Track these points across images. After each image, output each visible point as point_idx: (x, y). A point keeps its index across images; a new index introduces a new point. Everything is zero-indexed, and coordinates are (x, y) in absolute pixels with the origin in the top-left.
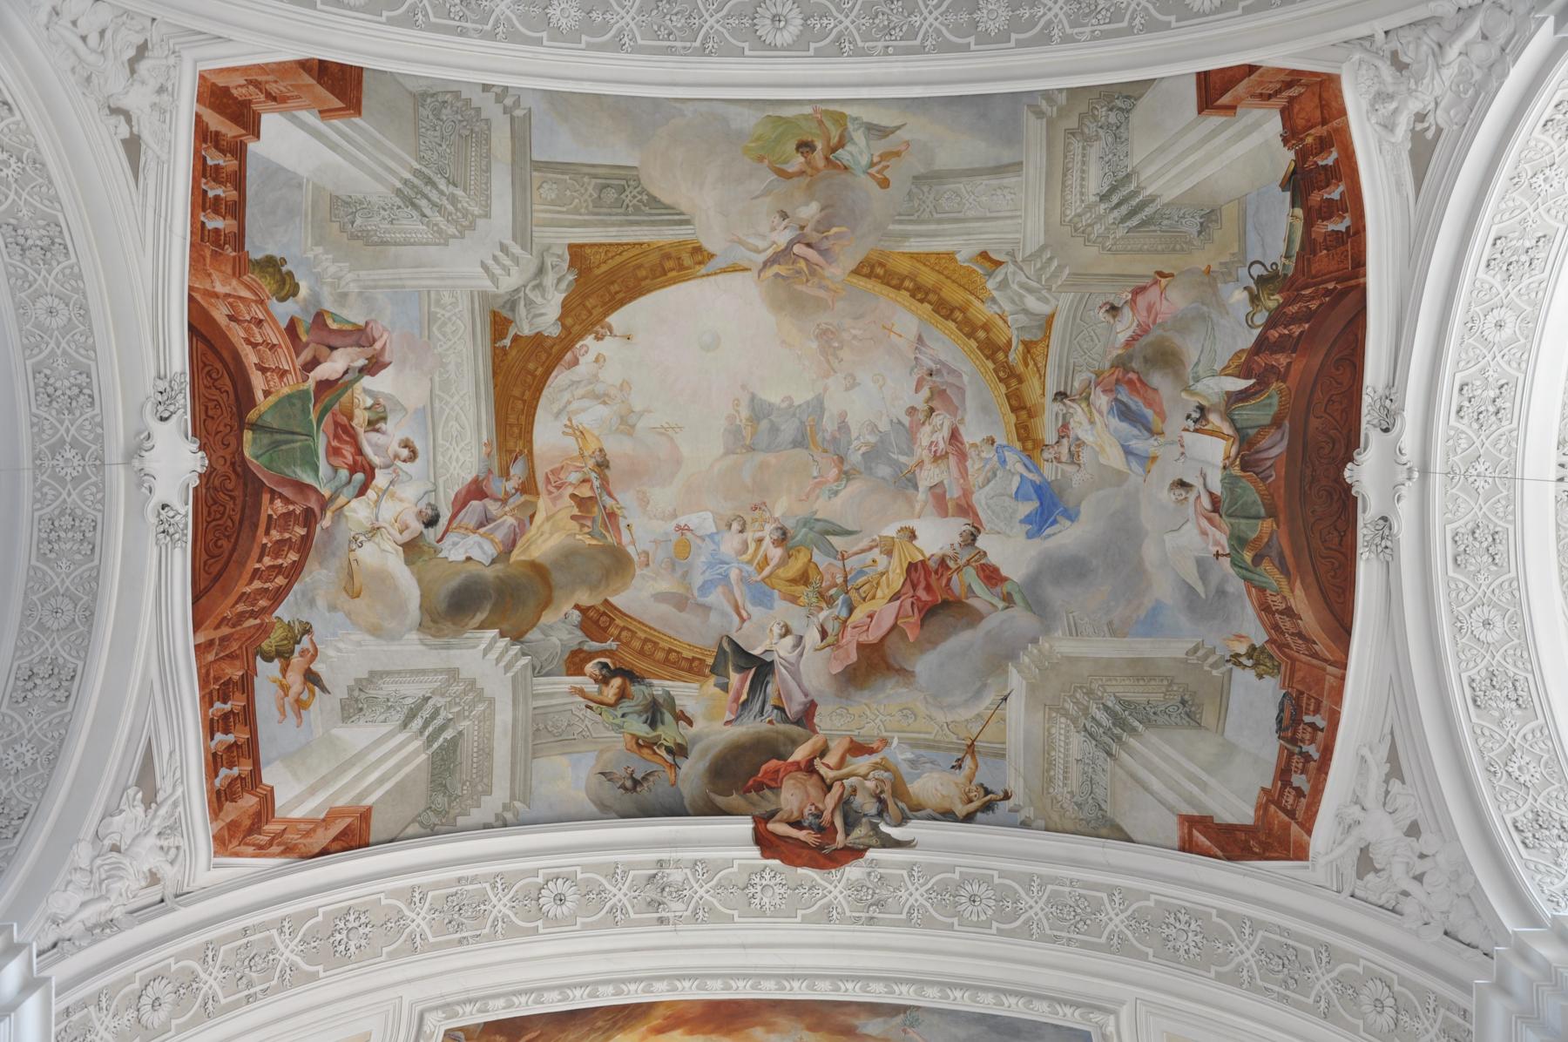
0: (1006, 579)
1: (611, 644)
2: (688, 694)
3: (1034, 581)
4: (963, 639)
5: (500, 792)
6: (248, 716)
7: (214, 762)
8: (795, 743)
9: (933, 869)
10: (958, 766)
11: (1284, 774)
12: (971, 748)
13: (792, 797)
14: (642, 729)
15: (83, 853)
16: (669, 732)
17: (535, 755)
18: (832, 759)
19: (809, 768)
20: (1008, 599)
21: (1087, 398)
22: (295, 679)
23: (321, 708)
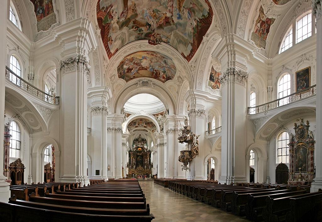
0: (174, 22)
1: (136, 24)
2: (143, 28)
3: (177, 24)
4: (170, 26)
8: (153, 33)
9: (162, 47)
10: (166, 38)
12: (168, 37)
13: (152, 38)
14: (139, 32)
16: (141, 32)
18: (156, 35)
19: (154, 35)
20: (174, 24)
21: (186, 9)
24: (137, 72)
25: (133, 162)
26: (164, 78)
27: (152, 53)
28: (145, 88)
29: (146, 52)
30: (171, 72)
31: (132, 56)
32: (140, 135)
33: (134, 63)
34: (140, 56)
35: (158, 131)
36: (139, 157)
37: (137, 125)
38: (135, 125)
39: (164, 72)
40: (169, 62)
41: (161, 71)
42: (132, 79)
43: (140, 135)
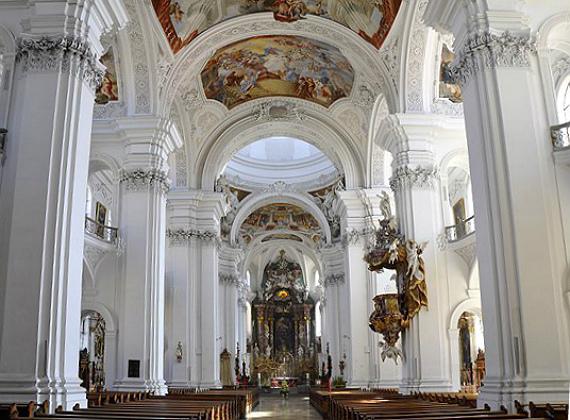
5: (221, 15)
6: (172, 27)
7: (169, 39)
11: (379, 32)
13: (281, 8)
15: (158, 72)
17: (227, 6)
22: (178, 15)
23: (184, 16)
24: (256, 85)
25: (264, 334)
26: (325, 94)
27: (288, 40)
28: (277, 124)
29: (272, 39)
30: (342, 79)
31: (238, 48)
32: (282, 252)
33: (246, 64)
34: (259, 48)
35: (325, 239)
36: (282, 319)
37: (270, 223)
38: (265, 222)
39: (325, 81)
40: (333, 55)
41: (317, 78)
42: (243, 101)
43: (282, 252)
